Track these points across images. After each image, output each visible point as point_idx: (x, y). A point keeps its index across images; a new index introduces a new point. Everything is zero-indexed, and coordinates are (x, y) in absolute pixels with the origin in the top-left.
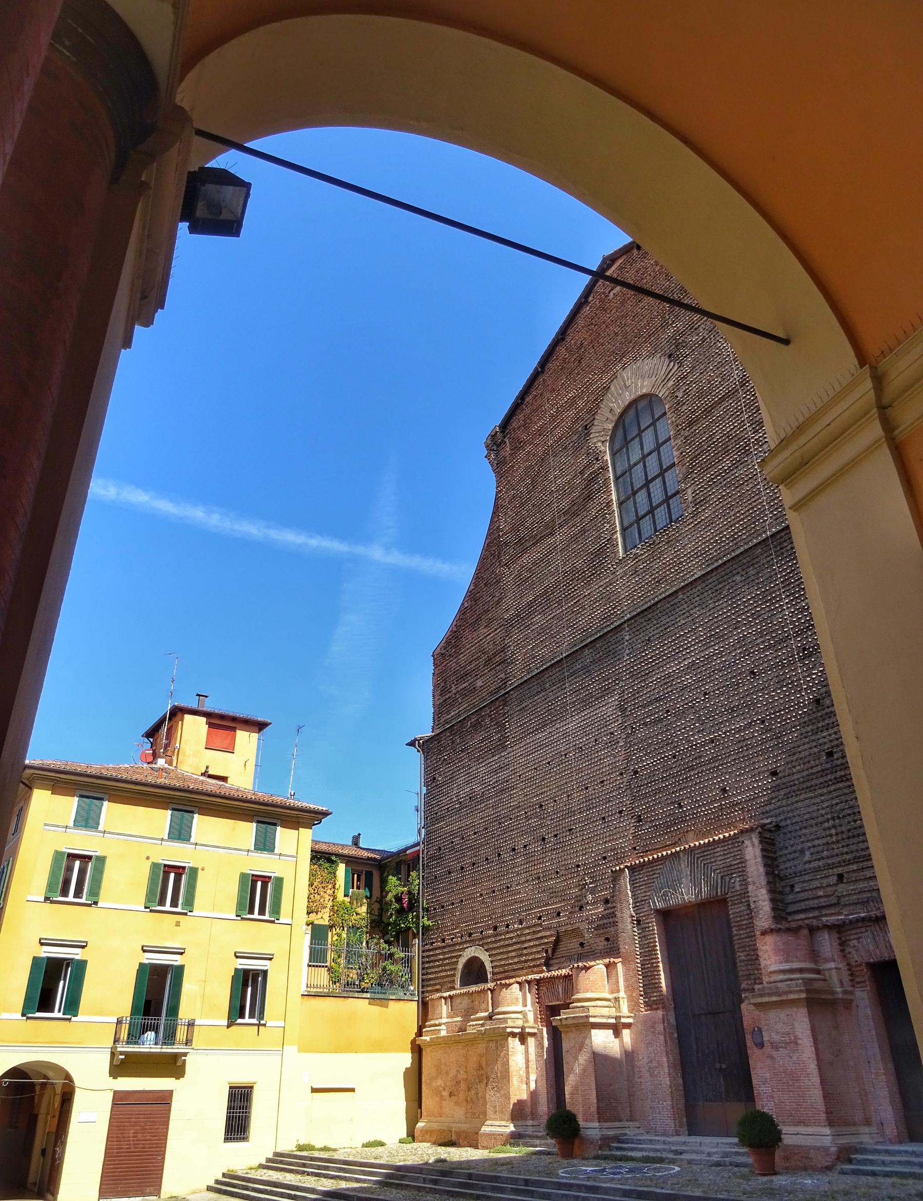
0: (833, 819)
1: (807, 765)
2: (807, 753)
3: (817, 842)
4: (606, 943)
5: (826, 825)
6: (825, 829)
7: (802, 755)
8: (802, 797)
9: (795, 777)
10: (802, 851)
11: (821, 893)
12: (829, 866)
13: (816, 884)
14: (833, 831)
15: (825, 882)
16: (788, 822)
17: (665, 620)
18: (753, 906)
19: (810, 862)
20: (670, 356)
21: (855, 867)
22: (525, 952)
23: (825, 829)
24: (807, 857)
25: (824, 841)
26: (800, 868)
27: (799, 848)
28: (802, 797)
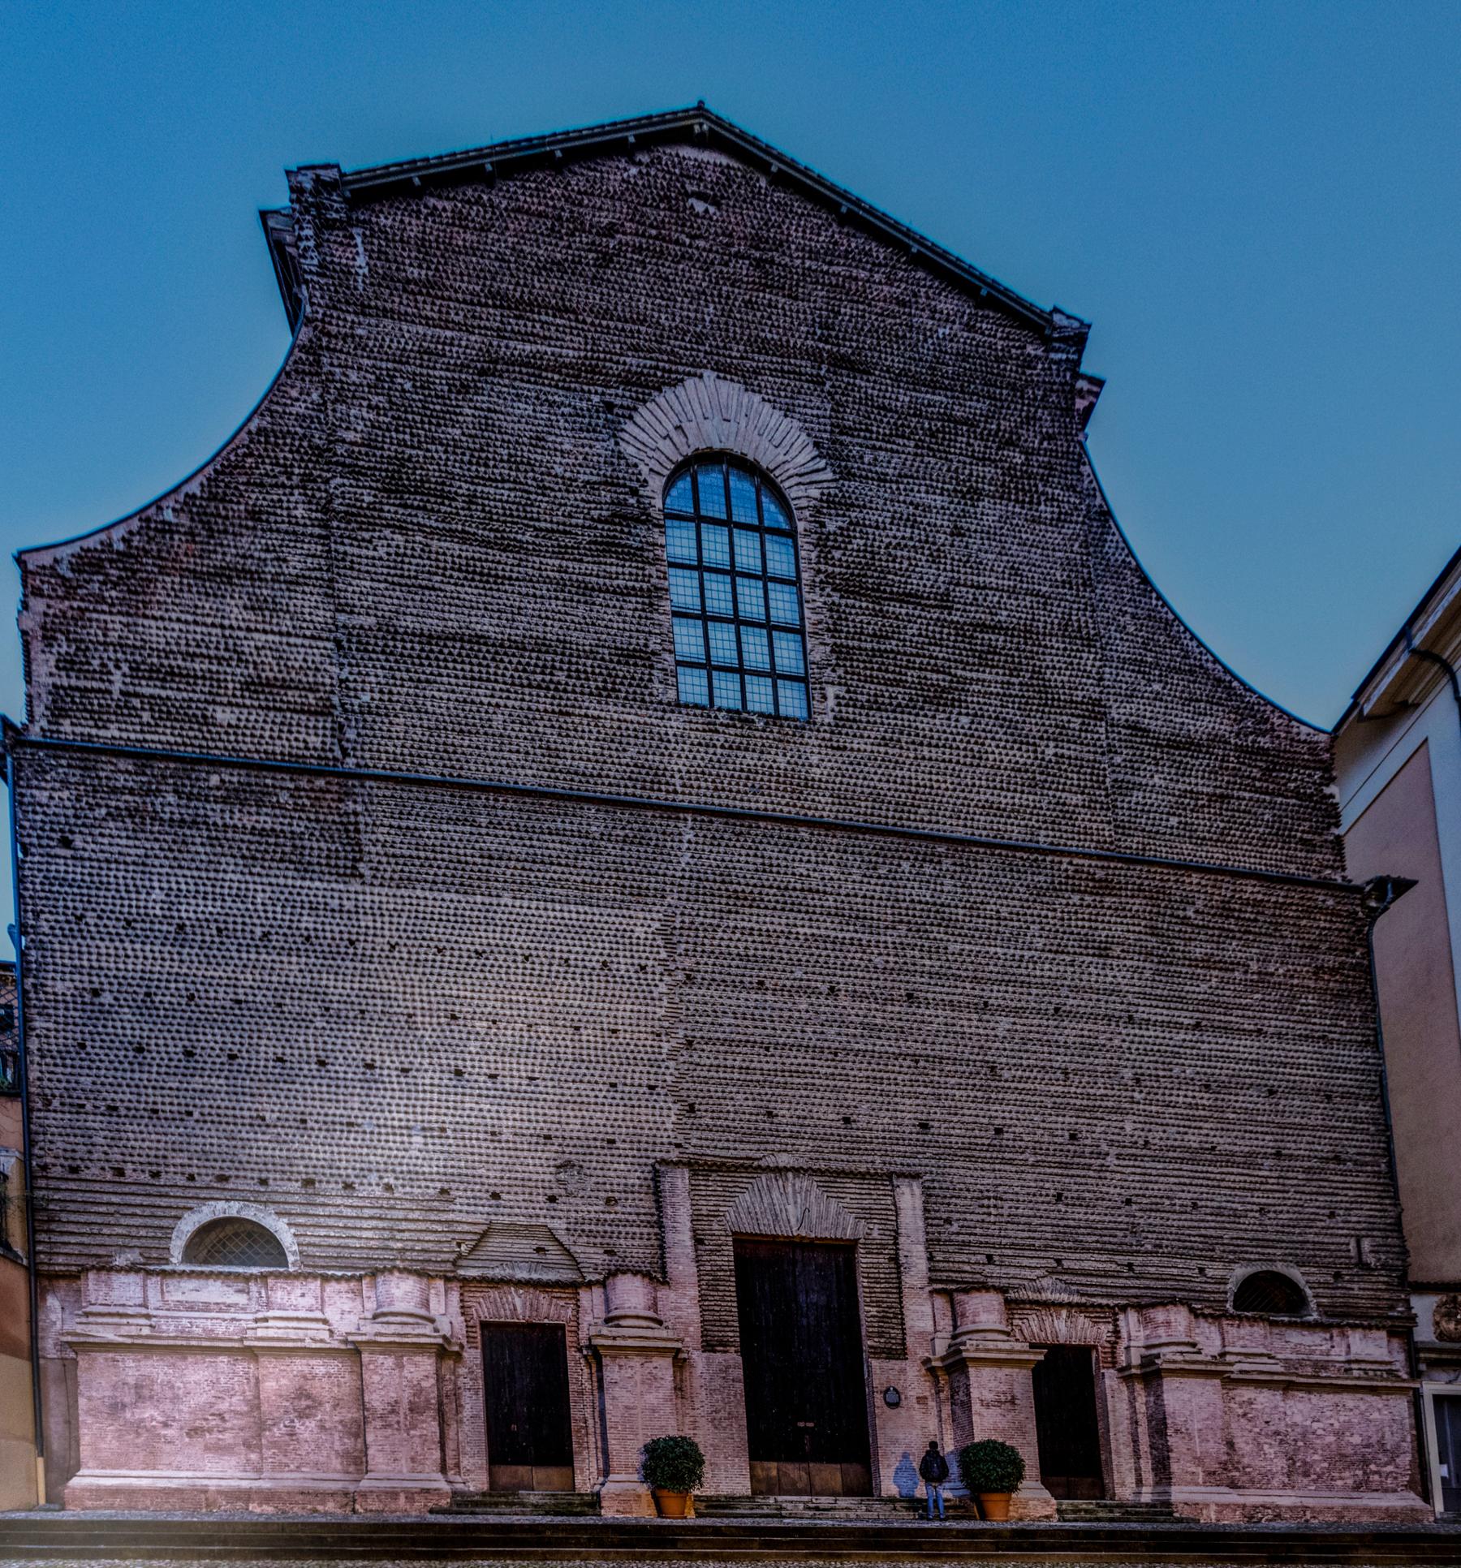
0: (996, 1198)
1: (969, 1133)
2: (971, 1119)
3: (968, 1216)
4: (606, 1257)
5: (986, 1202)
6: (982, 1206)
7: (965, 1119)
8: (958, 1164)
9: (953, 1140)
10: (948, 1221)
11: (967, 1268)
12: (980, 1244)
13: (964, 1258)
14: (993, 1211)
15: (973, 1259)
16: (936, 1184)
17: (771, 852)
18: (903, 1260)
19: (958, 1234)
20: (817, 445)
21: (1010, 1252)
22: (398, 1236)
23: (982, 1206)
24: (955, 1228)
25: (979, 1217)
26: (943, 1237)
27: (944, 1216)
28: (958, 1164)
